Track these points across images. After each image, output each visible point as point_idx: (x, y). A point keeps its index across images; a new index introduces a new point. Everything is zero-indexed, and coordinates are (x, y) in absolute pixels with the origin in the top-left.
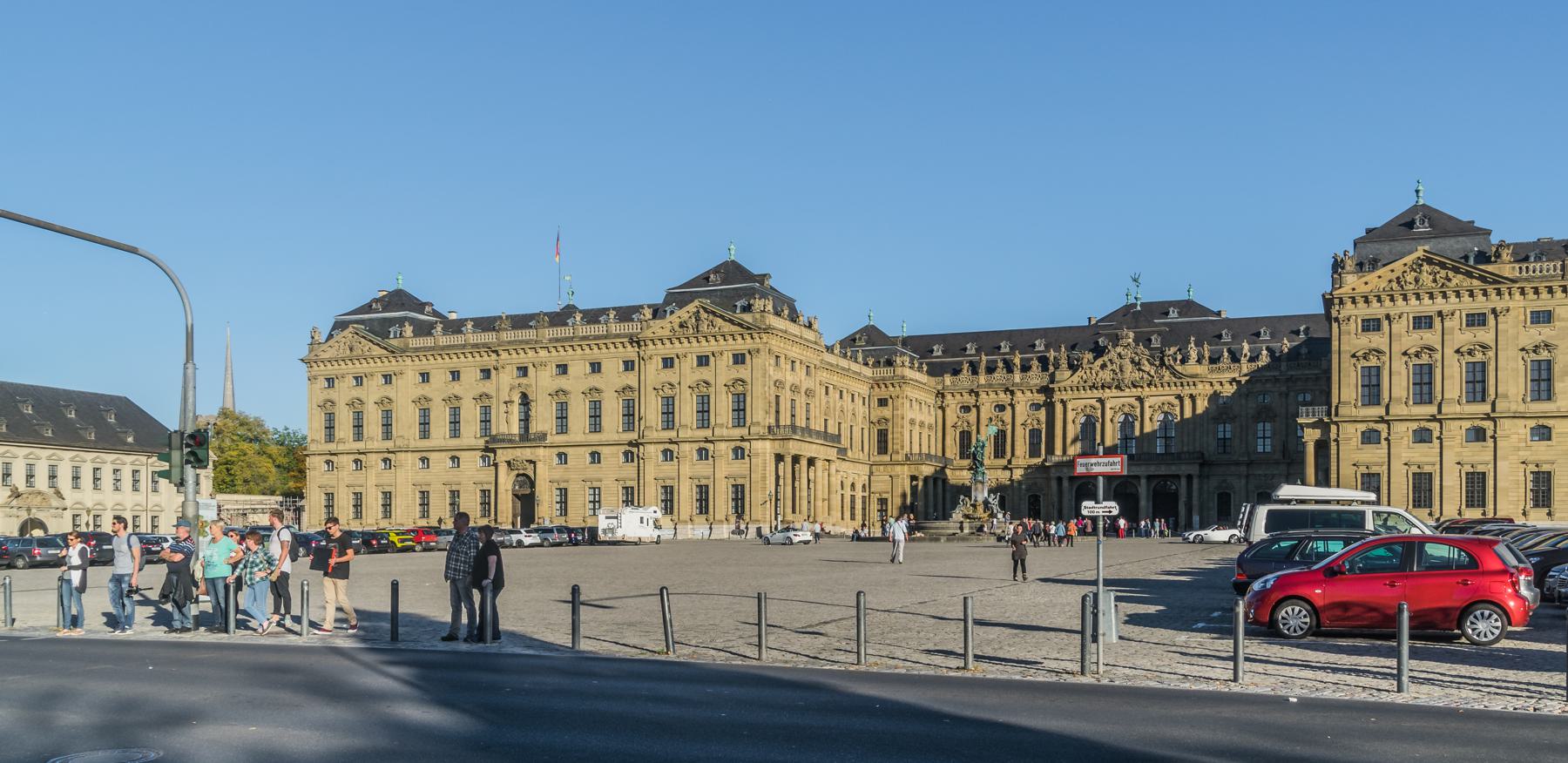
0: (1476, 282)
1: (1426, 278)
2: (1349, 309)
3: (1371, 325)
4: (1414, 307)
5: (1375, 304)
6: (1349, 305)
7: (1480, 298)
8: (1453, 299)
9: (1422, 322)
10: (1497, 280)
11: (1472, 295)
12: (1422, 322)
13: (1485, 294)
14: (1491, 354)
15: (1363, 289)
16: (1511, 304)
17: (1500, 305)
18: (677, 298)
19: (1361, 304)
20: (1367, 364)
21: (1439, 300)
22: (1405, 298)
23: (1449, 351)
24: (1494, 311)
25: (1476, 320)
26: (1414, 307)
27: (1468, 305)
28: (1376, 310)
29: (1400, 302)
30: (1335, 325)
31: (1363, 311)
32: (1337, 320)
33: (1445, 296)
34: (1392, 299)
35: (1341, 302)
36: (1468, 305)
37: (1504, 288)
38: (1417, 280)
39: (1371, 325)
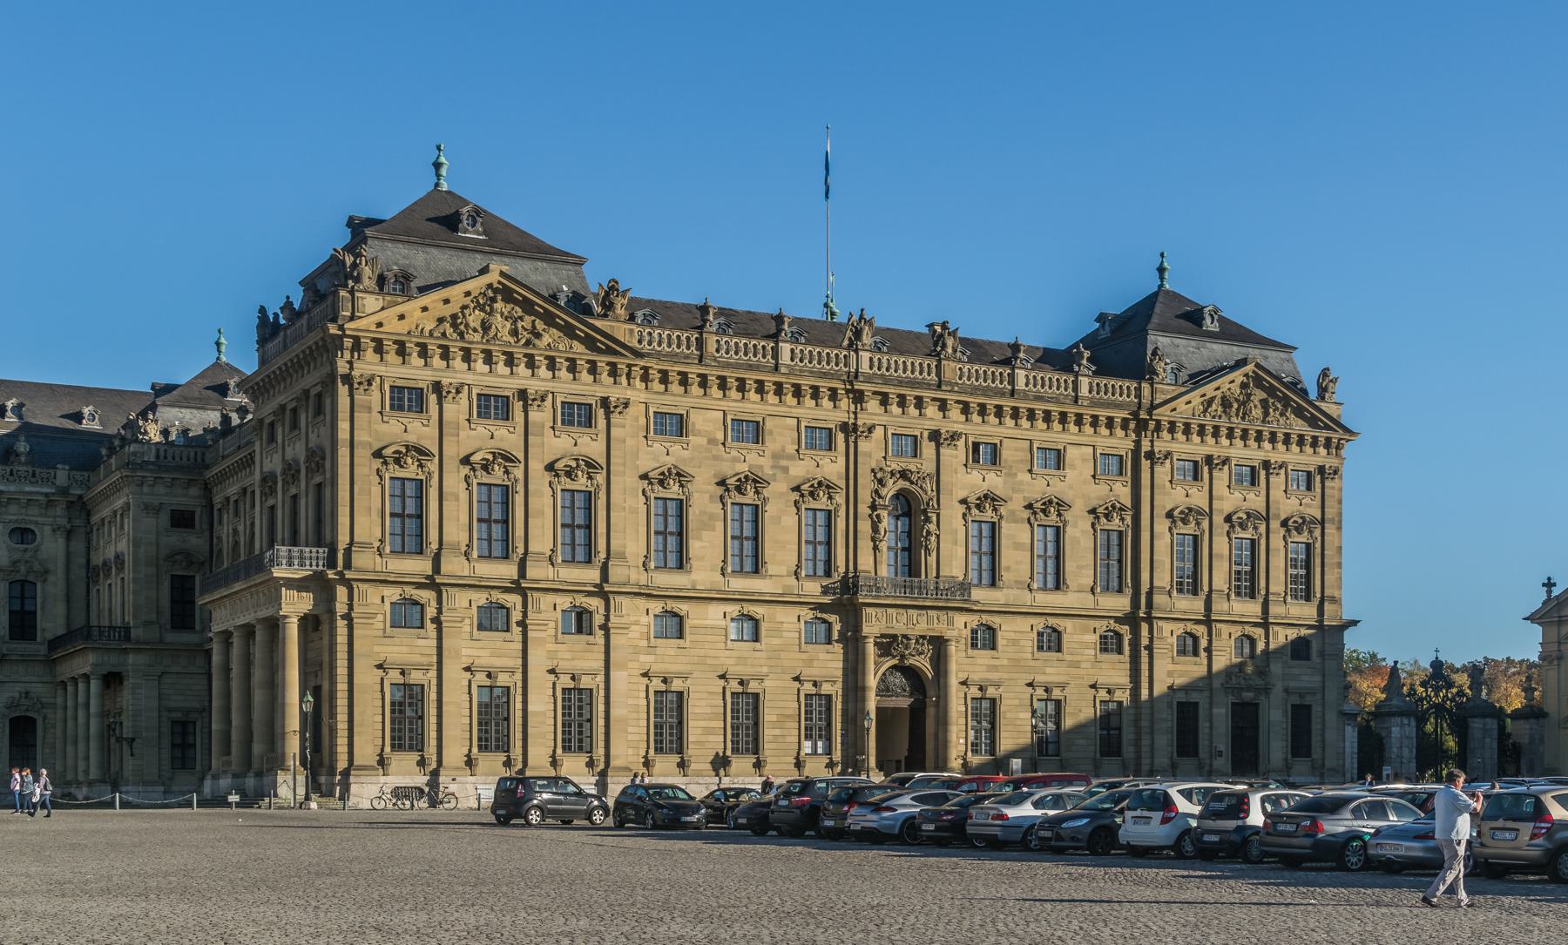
0: (578, 347)
1: (501, 326)
3: (407, 399)
4: (480, 377)
5: (415, 360)
6: (370, 355)
7: (585, 377)
8: (543, 372)
9: (493, 406)
10: (613, 347)
11: (573, 368)
12: (493, 406)
13: (593, 370)
14: (600, 478)
15: (393, 327)
16: (629, 394)
17: (615, 394)
19: (391, 357)
20: (401, 473)
21: (522, 370)
22: (467, 357)
24: (605, 402)
25: (578, 415)
26: (480, 377)
27: (566, 387)
28: (416, 372)
29: (458, 363)
30: (343, 390)
31: (393, 370)
32: (348, 379)
33: (531, 364)
34: (446, 355)
35: (357, 346)
36: (566, 387)
38: (486, 327)
39: (407, 399)
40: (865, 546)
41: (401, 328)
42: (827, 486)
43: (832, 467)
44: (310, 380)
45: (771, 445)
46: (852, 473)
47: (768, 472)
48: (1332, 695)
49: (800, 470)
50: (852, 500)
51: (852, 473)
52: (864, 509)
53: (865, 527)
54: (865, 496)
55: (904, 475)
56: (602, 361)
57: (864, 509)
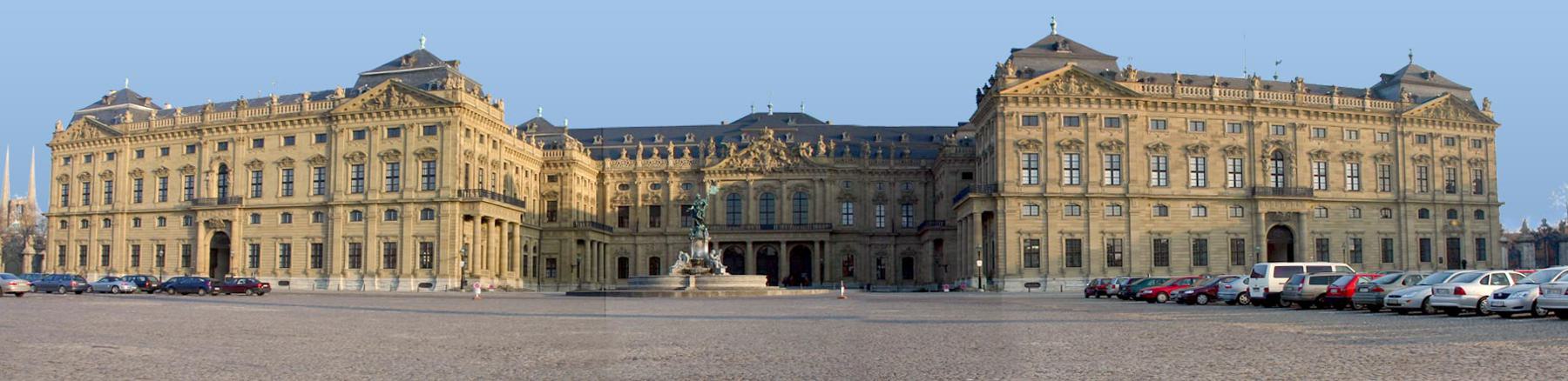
1: (1074, 87)
2: (1011, 108)
3: (1030, 121)
9: (1072, 121)
10: (1128, 93)
12: (1072, 121)
18: (369, 79)
23: (1092, 145)
25: (1113, 122)
28: (1033, 109)
31: (1023, 109)
37: (1133, 100)
38: (1067, 88)
39: (1030, 121)
40: (1259, 174)
41: (1026, 92)
42: (1241, 149)
43: (1242, 140)
44: (989, 116)
45: (1210, 132)
46: (1251, 143)
47: (1209, 143)
48: (1495, 234)
49: (1224, 142)
50: (1252, 155)
51: (1251, 143)
52: (1258, 158)
53: (1259, 166)
54: (1258, 152)
55: (1278, 142)
56: (1123, 100)
57: (1258, 158)
